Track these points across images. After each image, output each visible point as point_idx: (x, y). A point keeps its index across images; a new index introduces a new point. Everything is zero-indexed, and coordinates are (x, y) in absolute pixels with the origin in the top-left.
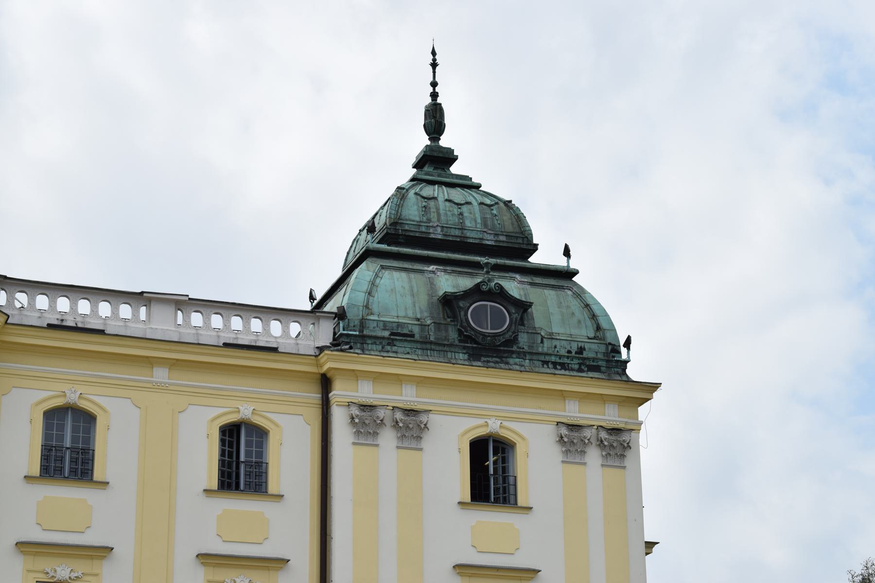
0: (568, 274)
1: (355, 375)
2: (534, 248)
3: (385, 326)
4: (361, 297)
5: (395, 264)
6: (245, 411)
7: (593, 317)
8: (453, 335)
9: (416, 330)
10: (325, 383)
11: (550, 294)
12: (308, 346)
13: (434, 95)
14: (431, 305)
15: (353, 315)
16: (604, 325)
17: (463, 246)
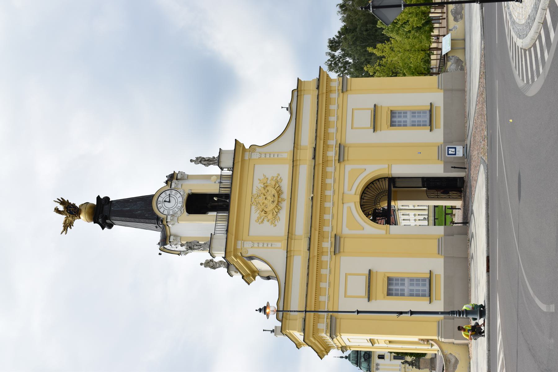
5: (361, 365)
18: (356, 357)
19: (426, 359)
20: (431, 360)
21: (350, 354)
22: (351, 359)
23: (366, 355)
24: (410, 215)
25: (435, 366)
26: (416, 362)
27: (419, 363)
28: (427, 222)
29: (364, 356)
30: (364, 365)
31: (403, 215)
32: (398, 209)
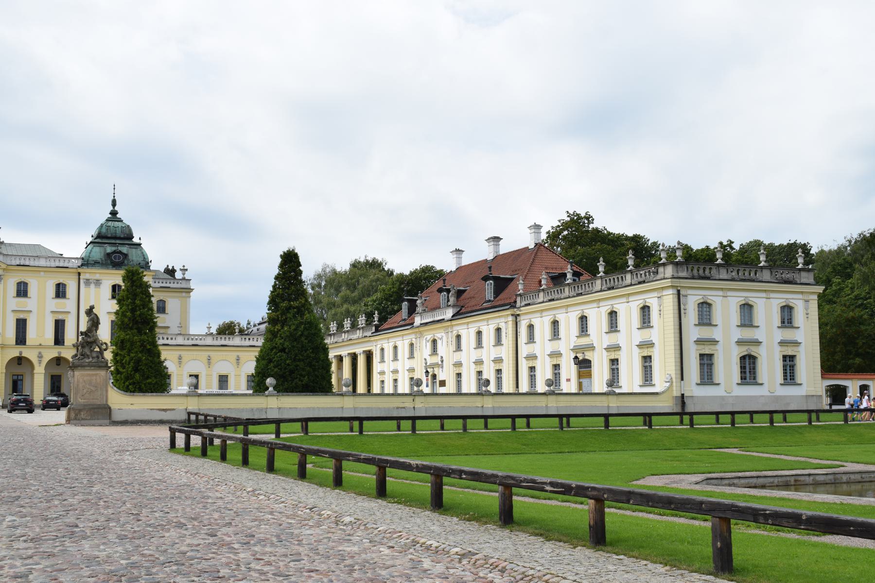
0: (140, 245)
1: (85, 273)
2: (133, 237)
3: (93, 261)
4: (88, 254)
5: (97, 245)
6: (61, 281)
7: (143, 255)
8: (109, 262)
9: (100, 261)
10: (79, 274)
11: (134, 250)
12: (75, 266)
13: (114, 197)
14: (104, 255)
15: (86, 259)
16: (146, 257)
17: (115, 238)
18: (116, 233)
19: (107, 391)
20: (105, 408)
21: (122, 221)
22: (110, 223)
23: (119, 258)
24: (395, 362)
25: (83, 422)
26: (94, 355)
27: (91, 366)
28: (474, 390)
29: (117, 253)
30: (98, 253)
31: (498, 330)
32: (518, 315)
